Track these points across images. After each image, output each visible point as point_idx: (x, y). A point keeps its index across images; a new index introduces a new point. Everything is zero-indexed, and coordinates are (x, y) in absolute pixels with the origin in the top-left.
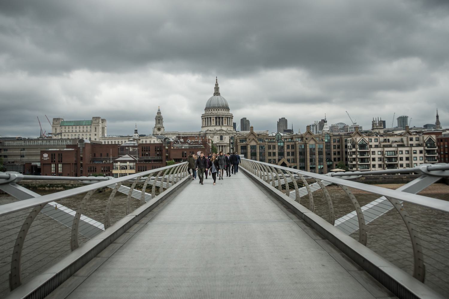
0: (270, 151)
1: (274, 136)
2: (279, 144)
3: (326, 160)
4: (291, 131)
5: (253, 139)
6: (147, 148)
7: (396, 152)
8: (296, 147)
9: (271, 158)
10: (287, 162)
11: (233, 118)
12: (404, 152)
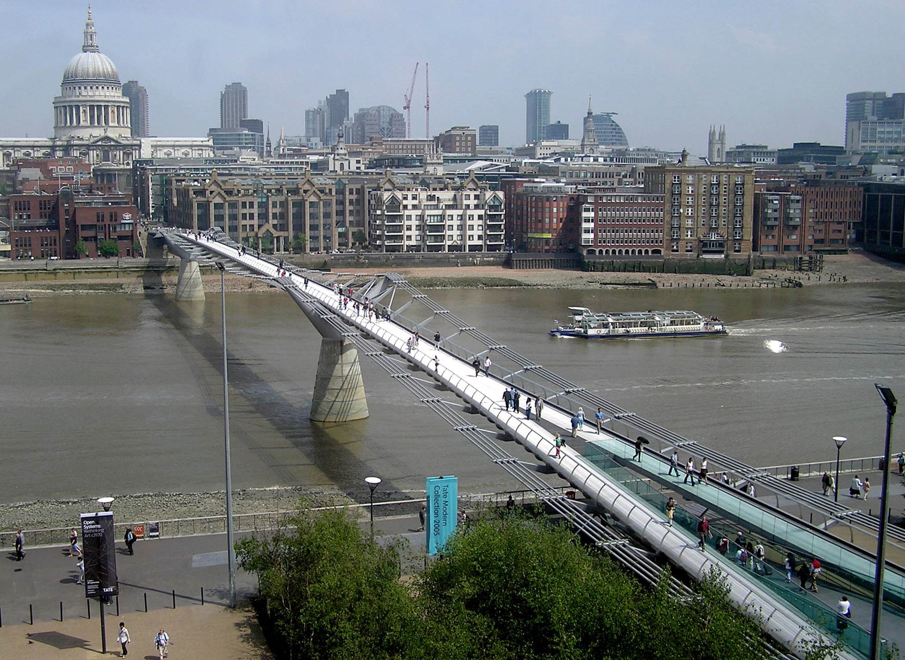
0: (245, 211)
2: (260, 200)
7: (442, 217)
9: (248, 222)
12: (455, 217)
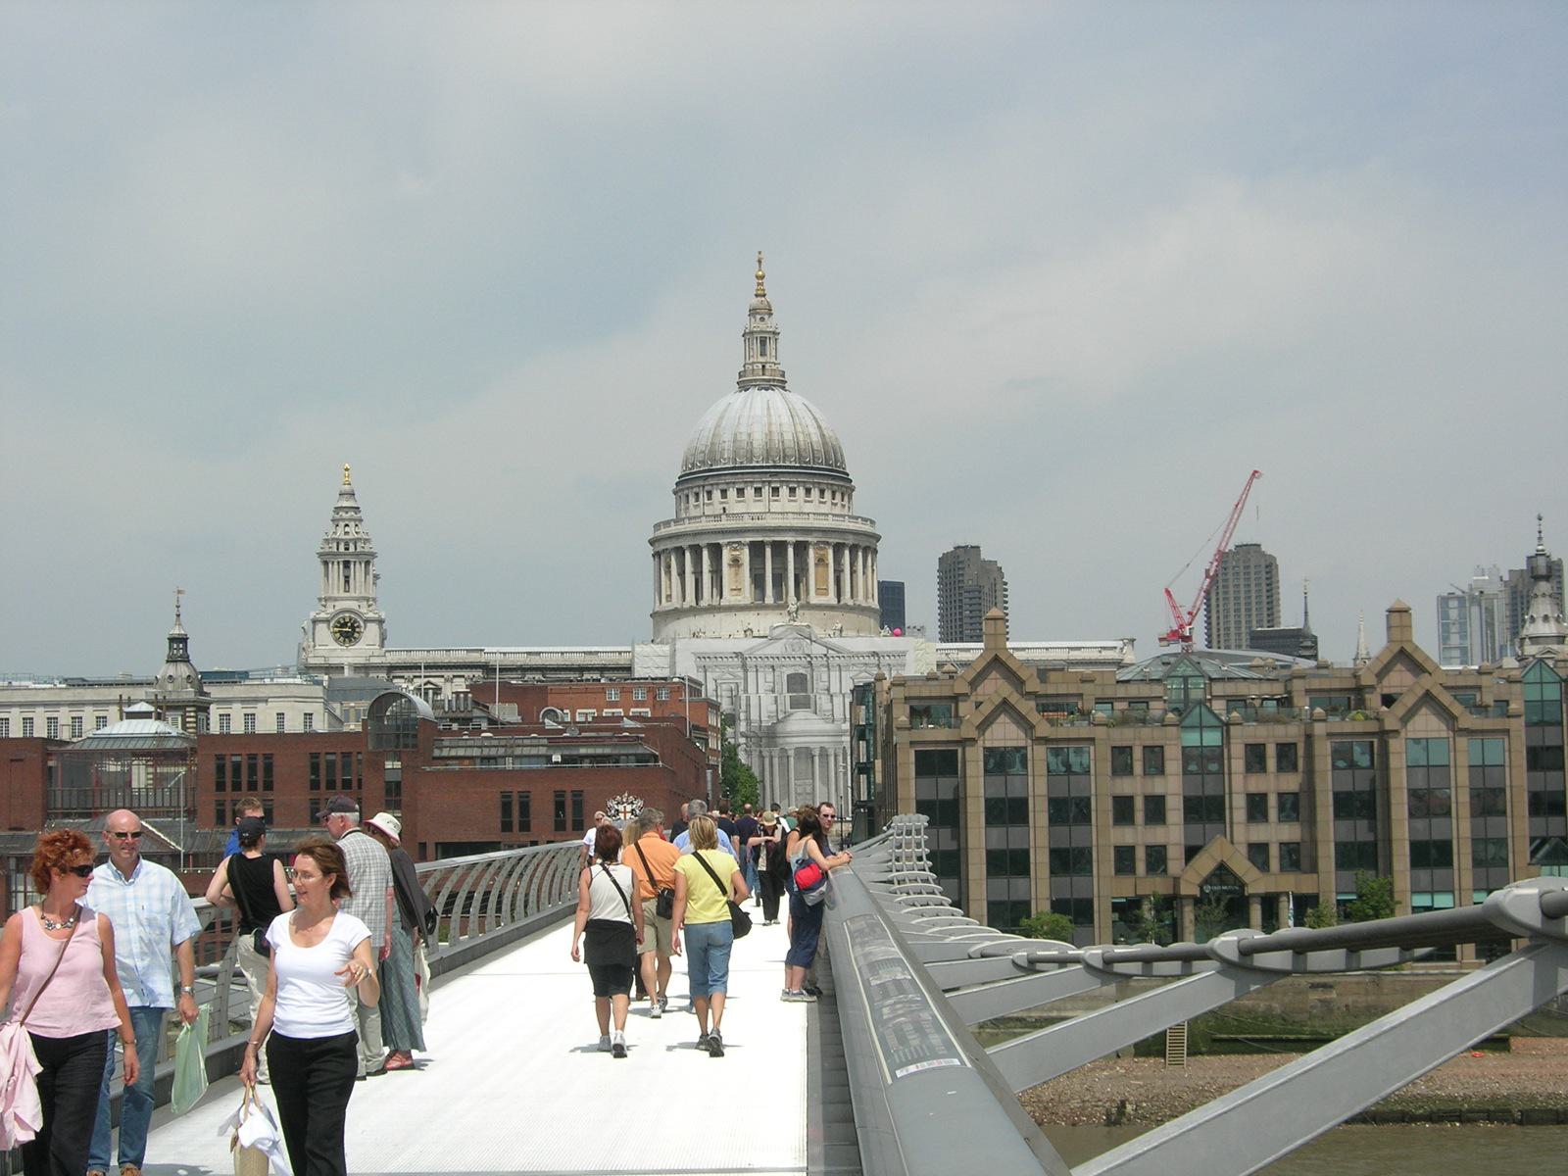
0: (1126, 786)
1: (1158, 681)
2: (1192, 739)
3: (1533, 853)
4: (1299, 642)
5: (1005, 701)
6: (252, 769)
8: (1310, 756)
9: (1138, 835)
10: (1249, 864)
11: (875, 551)
